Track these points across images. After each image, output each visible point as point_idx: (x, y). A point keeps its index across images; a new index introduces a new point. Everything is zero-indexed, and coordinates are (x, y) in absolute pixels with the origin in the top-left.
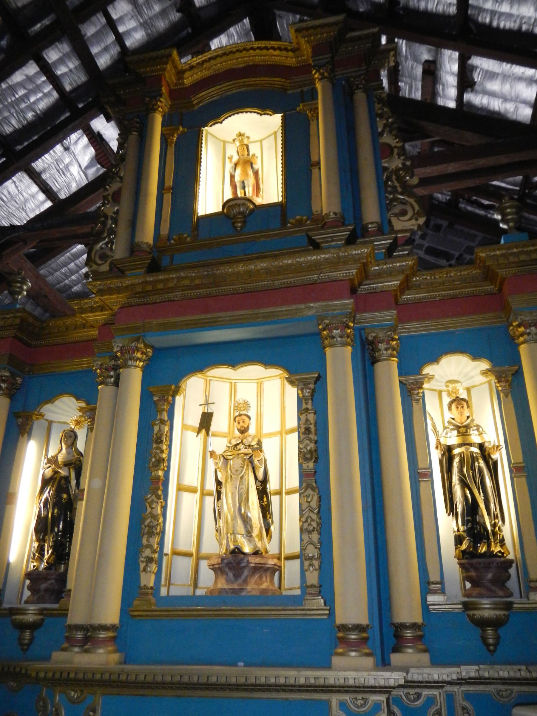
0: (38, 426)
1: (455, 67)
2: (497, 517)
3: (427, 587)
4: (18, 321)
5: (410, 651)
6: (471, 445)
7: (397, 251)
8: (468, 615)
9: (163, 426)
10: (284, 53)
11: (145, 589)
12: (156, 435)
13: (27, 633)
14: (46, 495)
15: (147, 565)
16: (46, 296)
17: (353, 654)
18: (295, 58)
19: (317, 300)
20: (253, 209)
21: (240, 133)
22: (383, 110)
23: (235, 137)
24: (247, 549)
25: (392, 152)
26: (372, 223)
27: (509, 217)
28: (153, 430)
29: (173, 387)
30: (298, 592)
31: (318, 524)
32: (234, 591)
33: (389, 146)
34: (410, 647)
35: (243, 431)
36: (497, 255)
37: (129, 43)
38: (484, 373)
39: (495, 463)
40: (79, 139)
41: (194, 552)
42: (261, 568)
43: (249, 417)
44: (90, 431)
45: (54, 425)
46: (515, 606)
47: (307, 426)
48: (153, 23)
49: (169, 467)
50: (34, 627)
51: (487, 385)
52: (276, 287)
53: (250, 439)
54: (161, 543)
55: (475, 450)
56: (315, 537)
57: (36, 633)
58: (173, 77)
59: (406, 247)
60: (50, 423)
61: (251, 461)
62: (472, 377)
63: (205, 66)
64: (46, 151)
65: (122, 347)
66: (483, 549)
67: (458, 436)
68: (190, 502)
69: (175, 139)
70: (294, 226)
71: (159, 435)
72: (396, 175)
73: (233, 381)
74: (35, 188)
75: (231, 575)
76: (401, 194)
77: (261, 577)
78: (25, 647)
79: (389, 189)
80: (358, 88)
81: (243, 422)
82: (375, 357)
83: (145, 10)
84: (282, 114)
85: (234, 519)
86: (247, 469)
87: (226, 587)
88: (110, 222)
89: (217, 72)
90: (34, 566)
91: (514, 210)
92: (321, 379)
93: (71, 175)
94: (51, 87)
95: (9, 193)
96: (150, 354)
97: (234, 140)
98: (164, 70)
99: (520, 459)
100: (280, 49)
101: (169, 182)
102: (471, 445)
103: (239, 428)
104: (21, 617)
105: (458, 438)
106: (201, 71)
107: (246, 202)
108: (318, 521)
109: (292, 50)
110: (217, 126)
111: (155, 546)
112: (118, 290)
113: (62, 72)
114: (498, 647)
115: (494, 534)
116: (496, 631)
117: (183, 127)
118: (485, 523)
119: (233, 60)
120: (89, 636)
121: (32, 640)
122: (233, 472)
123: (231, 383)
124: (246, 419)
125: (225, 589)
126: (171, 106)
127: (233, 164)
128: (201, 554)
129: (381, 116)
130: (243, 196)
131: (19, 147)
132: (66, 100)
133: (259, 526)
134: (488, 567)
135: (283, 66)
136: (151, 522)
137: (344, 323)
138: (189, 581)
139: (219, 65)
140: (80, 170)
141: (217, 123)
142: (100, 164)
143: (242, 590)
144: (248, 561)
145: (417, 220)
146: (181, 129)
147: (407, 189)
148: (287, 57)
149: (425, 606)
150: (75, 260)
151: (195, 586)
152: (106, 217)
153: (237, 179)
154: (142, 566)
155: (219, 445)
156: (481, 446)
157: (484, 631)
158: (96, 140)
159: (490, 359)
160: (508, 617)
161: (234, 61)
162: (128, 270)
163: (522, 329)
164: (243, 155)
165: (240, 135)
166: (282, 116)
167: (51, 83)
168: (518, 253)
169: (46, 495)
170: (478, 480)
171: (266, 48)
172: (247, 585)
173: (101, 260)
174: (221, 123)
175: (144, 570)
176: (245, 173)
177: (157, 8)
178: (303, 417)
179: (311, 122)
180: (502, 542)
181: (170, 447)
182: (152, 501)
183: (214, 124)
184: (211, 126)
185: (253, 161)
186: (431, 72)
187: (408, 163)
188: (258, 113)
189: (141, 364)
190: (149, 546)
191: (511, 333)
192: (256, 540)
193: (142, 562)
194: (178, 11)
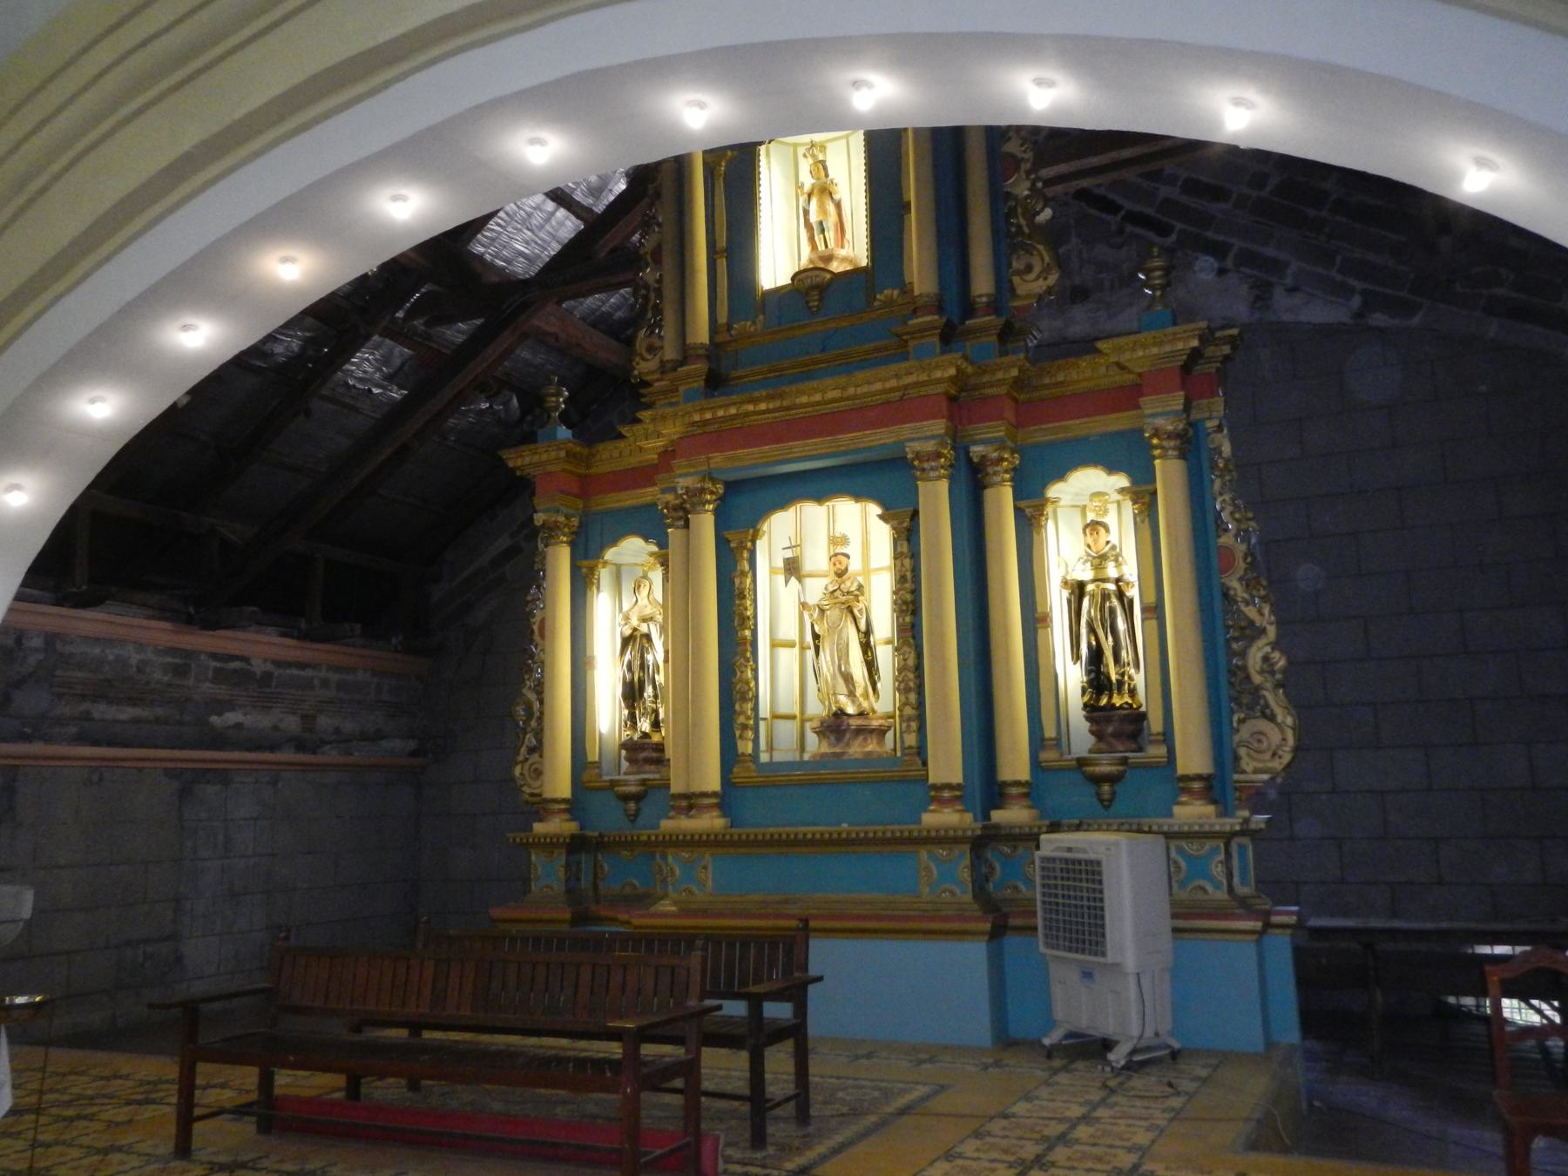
0: (604, 575)
4: (563, 454)
6: (1104, 580)
8: (1084, 773)
14: (627, 657)
16: (579, 345)
24: (850, 710)
32: (835, 754)
35: (841, 574)
38: (1122, 491)
39: (1131, 601)
43: (848, 556)
49: (756, 625)
50: (638, 798)
53: (848, 583)
54: (756, 708)
55: (1112, 587)
56: (913, 697)
61: (850, 610)
66: (1104, 701)
68: (788, 660)
75: (832, 738)
85: (834, 677)
88: (652, 295)
92: (915, 514)
101: (722, 242)
108: (913, 679)
115: (1120, 683)
120: (691, 802)
121: (638, 811)
124: (844, 559)
134: (1109, 720)
138: (795, 745)
149: (1035, 763)
151: (802, 748)
153: (813, 218)
154: (738, 733)
155: (816, 590)
169: (627, 657)
176: (822, 209)
180: (1133, 692)
181: (755, 601)
190: (743, 712)
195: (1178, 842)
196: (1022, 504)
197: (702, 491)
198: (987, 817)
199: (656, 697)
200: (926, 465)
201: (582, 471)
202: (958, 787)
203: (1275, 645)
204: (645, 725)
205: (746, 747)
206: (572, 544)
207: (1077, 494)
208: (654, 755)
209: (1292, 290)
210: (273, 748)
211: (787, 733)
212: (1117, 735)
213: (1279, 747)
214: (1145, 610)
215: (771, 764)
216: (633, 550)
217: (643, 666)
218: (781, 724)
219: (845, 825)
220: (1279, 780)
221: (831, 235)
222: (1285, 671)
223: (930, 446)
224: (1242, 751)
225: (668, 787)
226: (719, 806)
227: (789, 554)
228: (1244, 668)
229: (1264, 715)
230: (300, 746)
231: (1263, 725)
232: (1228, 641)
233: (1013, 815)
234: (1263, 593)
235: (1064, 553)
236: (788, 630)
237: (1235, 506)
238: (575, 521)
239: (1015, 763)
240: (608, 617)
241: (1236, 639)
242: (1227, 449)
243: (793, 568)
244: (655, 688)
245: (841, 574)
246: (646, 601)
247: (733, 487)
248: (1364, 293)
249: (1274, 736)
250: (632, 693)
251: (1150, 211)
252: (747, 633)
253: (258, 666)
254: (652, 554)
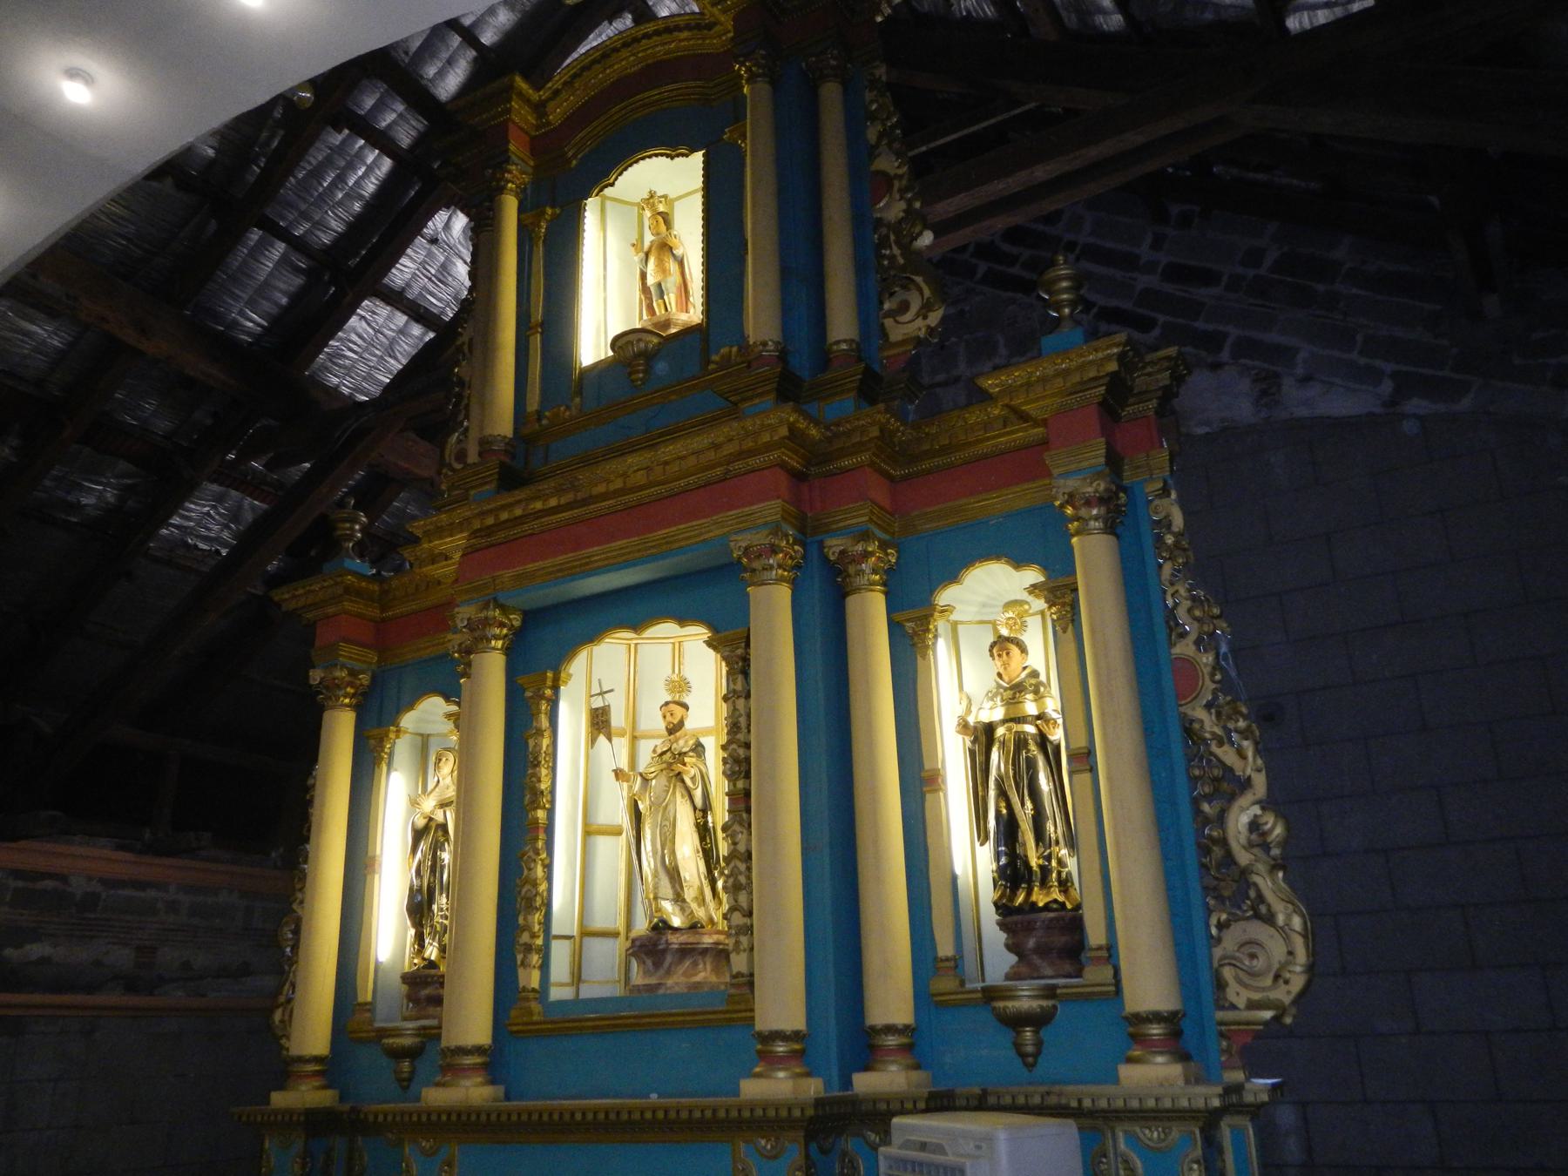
0: (402, 749)
2: (1057, 843)
4: (340, 591)
5: (893, 1068)
14: (419, 855)
17: (781, 1074)
24: (676, 922)
25: (891, 186)
29: (550, 675)
32: (651, 989)
34: (893, 1062)
35: (674, 729)
37: (488, 38)
38: (1034, 589)
40: (450, 218)
41: (622, 929)
42: (694, 950)
43: (686, 707)
45: (432, 739)
49: (553, 802)
50: (413, 1054)
53: (681, 742)
64: (400, 253)
74: (401, 319)
75: (649, 962)
77: (695, 964)
85: (656, 875)
86: (674, 793)
95: (360, 337)
96: (517, 623)
98: (509, 111)
101: (538, 314)
104: (391, 1041)
111: (537, 927)
112: (451, 529)
115: (1046, 871)
117: (553, 207)
124: (679, 711)
126: (535, 168)
127: (642, 255)
131: (352, 263)
132: (407, 164)
133: (697, 883)
134: (1029, 928)
146: (549, 211)
148: (704, 39)
149: (923, 997)
153: (651, 281)
154: (519, 957)
160: (1055, 1007)
174: (612, 185)
180: (1064, 884)
181: (554, 769)
188: (667, 156)
189: (500, 644)
190: (527, 928)
192: (694, 906)
195: (1127, 1126)
196: (898, 617)
197: (486, 622)
198: (847, 1083)
200: (756, 565)
201: (373, 612)
202: (796, 1036)
203: (1265, 805)
204: (432, 952)
206: (360, 710)
207: (984, 605)
209: (1306, 380)
210: (91, 989)
211: (606, 961)
212: (1042, 951)
213: (1283, 966)
215: (576, 1001)
216: (430, 714)
218: (597, 947)
219: (654, 1096)
220: (1288, 1020)
221: (672, 298)
222: (1285, 843)
223: (760, 538)
224: (1227, 973)
225: (438, 1037)
226: (485, 1067)
228: (1223, 842)
229: (1257, 916)
230: (131, 985)
231: (1258, 930)
232: (1196, 802)
233: (885, 1079)
234: (1242, 724)
235: (961, 687)
236: (614, 807)
237: (1194, 599)
238: (365, 679)
239: (891, 998)
240: (399, 801)
241: (1209, 798)
242: (1178, 521)
245: (674, 729)
247: (534, 618)
248: (1395, 375)
249: (1276, 949)
250: (419, 908)
251: (1127, 305)
252: (541, 814)
253: (78, 886)
254: (449, 716)
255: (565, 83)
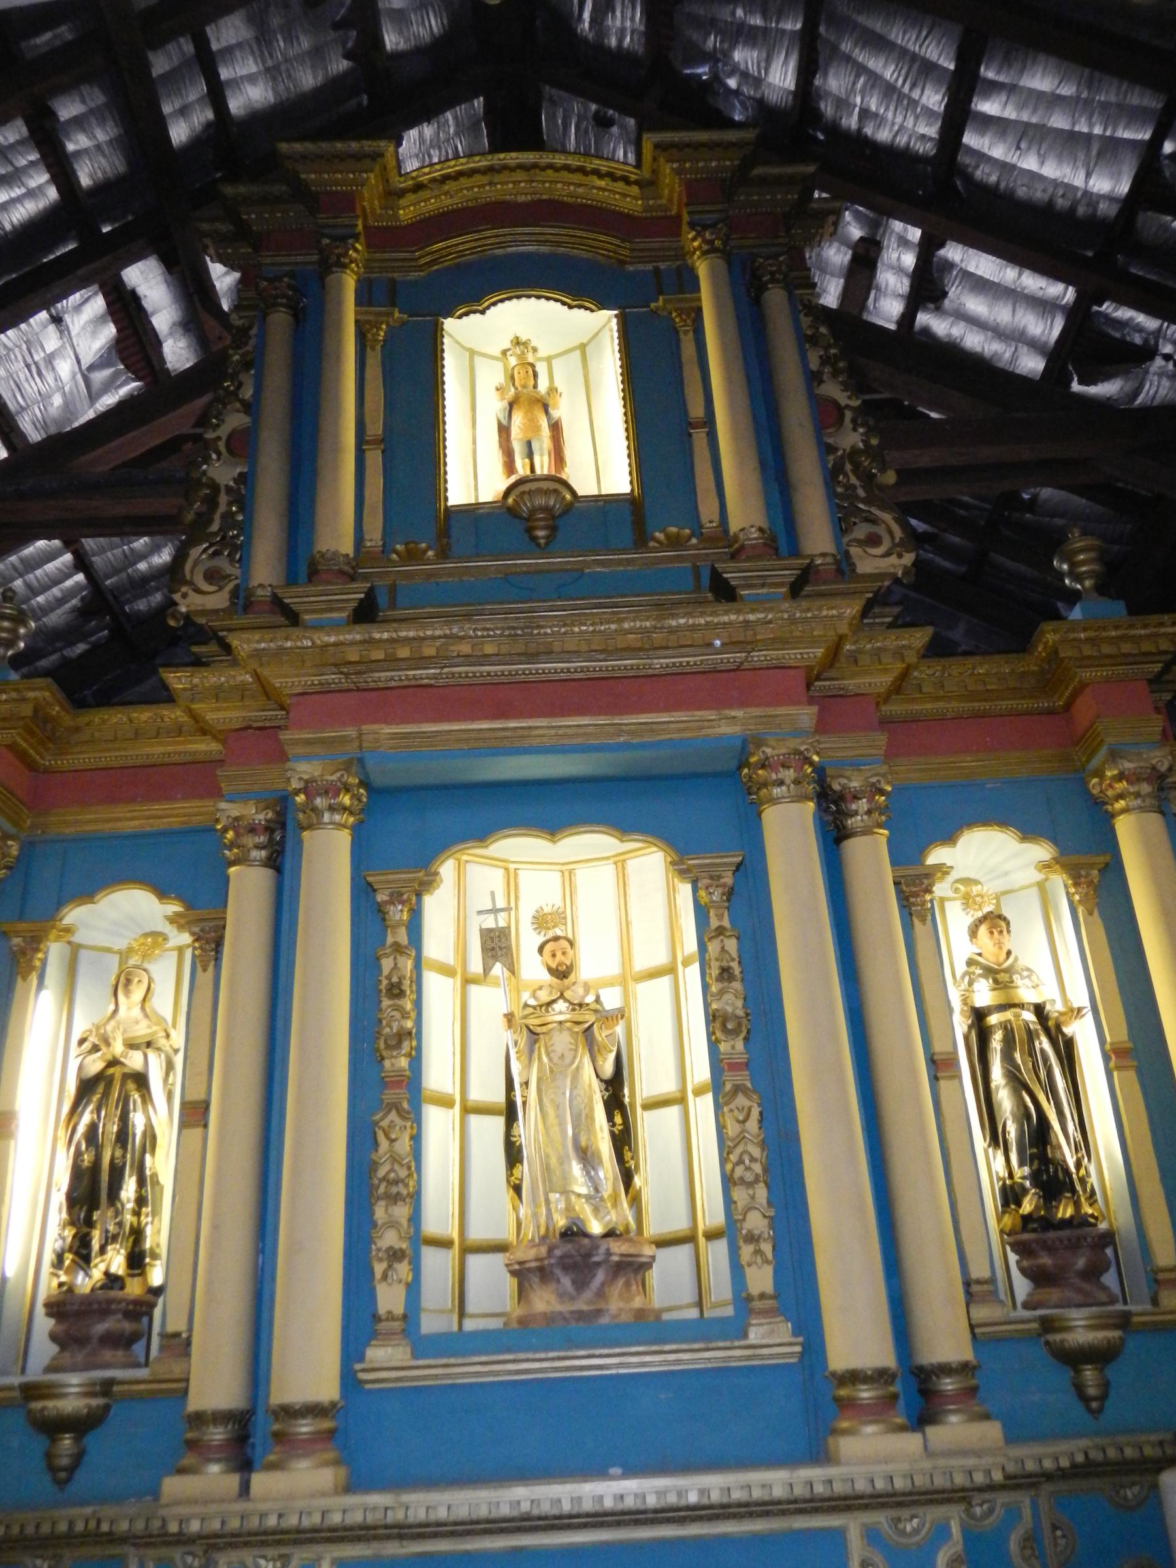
0: (54, 952)
1: (909, 260)
3: (974, 1290)
4: (27, 710)
5: (953, 1419)
7: (870, 615)
8: (1047, 1343)
9: (404, 958)
10: (620, 186)
11: (387, 1320)
12: (389, 977)
13: (67, 1442)
14: (87, 1118)
15: (390, 1266)
17: (870, 1429)
18: (641, 198)
19: (742, 704)
20: (572, 503)
21: (517, 338)
22: (817, 329)
23: (507, 345)
24: (596, 1228)
26: (823, 555)
27: (1084, 569)
28: (379, 969)
30: (729, 1311)
31: (766, 1170)
32: (580, 1316)
33: (835, 403)
36: (1081, 640)
37: (236, 105)
38: (1045, 866)
39: (1070, 1043)
40: (87, 300)
41: (455, 1236)
42: (630, 1264)
44: (199, 969)
45: (84, 955)
46: (1135, 1319)
47: (725, 964)
48: (292, 72)
51: (1035, 890)
52: (657, 672)
55: (1029, 1016)
57: (90, 1440)
58: (376, 202)
59: (887, 610)
60: (75, 949)
62: (1006, 874)
63: (446, 188)
65: (307, 782)
66: (1065, 1211)
67: (994, 989)
69: (382, 333)
70: (662, 546)
71: (395, 979)
72: (851, 463)
73: (512, 866)
75: (566, 1282)
76: (863, 501)
77: (628, 1285)
78: (62, 1475)
79: (839, 490)
80: (773, 280)
81: (564, 953)
82: (844, 827)
83: (282, 44)
84: (616, 312)
87: (559, 1307)
88: (223, 499)
89: (470, 204)
90: (61, 1285)
91: (1092, 555)
93: (56, 380)
94: (46, 177)
97: (504, 352)
99: (1123, 1035)
100: (611, 176)
101: (375, 428)
102: (1022, 1006)
103: (554, 966)
105: (996, 993)
106: (435, 197)
107: (557, 486)
108: (770, 1158)
109: (636, 183)
110: (475, 318)
113: (78, 147)
114: (1107, 1403)
116: (1101, 1370)
118: (1065, 1161)
119: (507, 183)
121: (78, 1458)
122: (555, 1060)
123: (507, 869)
125: (561, 1313)
127: (505, 404)
128: (468, 1243)
129: (813, 340)
130: (528, 472)
132: (74, 210)
134: (1074, 1246)
135: (614, 212)
136: (392, 1170)
137: (801, 753)
139: (476, 190)
140: (77, 370)
141: (475, 312)
142: (123, 361)
143: (599, 1312)
144: (608, 1250)
145: (900, 556)
146: (397, 315)
147: (876, 494)
148: (625, 195)
150: (28, 573)
151: (462, 1314)
152: (215, 487)
154: (379, 1268)
156: (1039, 1010)
157: (1078, 1371)
158: (126, 309)
159: (1055, 841)
161: (511, 186)
162: (307, 612)
163: (1121, 786)
164: (524, 386)
165: (517, 342)
166: (616, 316)
167: (49, 168)
168: (1117, 637)
169: (87, 1118)
170: (1043, 1074)
171: (582, 170)
172: (607, 1303)
173: (211, 584)
174: (483, 312)
175: (385, 1277)
177: (305, 43)
178: (713, 948)
179: (682, 336)
181: (418, 1004)
182: (392, 1125)
183: (467, 314)
184: (460, 317)
185: (551, 403)
186: (865, 259)
187: (874, 442)
188: (564, 303)
189: (351, 819)
191: (1095, 792)
193: (380, 1260)
194: (347, 56)
199: (141, 1201)
204: (116, 1261)
205: (390, 1299)
208: (128, 1326)
214: (1114, 1056)
216: (128, 913)
217: (123, 1137)
227: (489, 922)
243: (497, 945)
244: (141, 1182)
246: (136, 1012)
255: (434, 180)
